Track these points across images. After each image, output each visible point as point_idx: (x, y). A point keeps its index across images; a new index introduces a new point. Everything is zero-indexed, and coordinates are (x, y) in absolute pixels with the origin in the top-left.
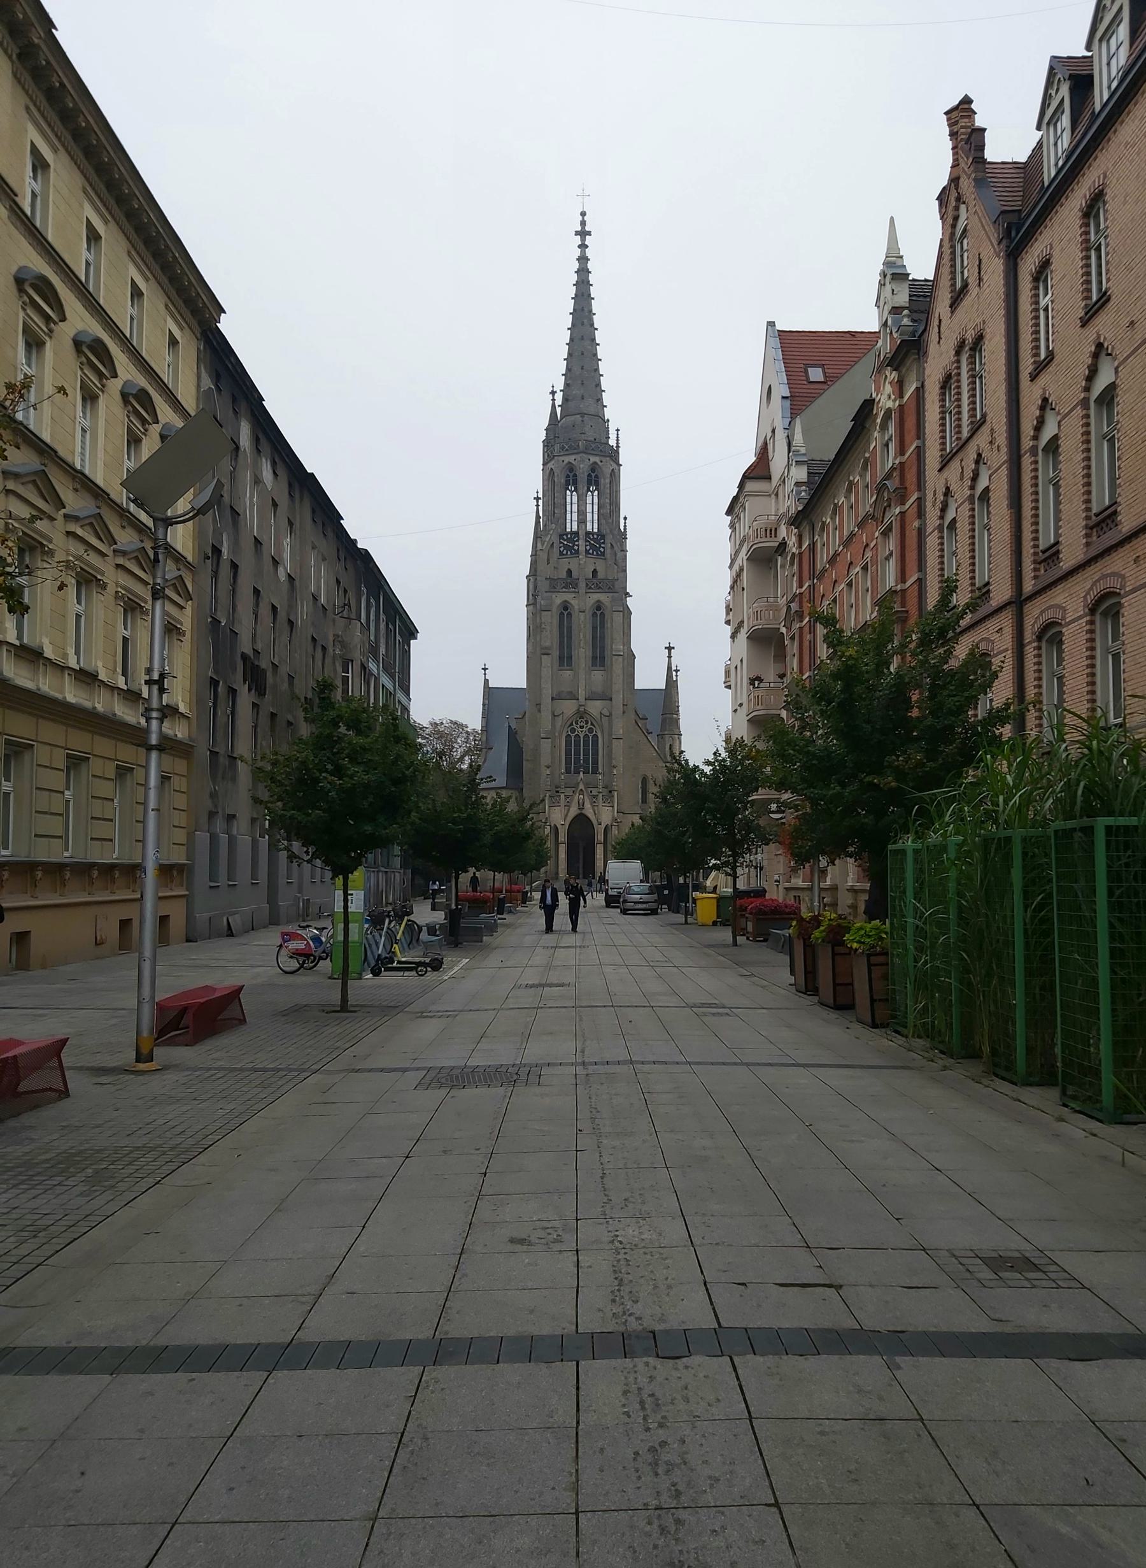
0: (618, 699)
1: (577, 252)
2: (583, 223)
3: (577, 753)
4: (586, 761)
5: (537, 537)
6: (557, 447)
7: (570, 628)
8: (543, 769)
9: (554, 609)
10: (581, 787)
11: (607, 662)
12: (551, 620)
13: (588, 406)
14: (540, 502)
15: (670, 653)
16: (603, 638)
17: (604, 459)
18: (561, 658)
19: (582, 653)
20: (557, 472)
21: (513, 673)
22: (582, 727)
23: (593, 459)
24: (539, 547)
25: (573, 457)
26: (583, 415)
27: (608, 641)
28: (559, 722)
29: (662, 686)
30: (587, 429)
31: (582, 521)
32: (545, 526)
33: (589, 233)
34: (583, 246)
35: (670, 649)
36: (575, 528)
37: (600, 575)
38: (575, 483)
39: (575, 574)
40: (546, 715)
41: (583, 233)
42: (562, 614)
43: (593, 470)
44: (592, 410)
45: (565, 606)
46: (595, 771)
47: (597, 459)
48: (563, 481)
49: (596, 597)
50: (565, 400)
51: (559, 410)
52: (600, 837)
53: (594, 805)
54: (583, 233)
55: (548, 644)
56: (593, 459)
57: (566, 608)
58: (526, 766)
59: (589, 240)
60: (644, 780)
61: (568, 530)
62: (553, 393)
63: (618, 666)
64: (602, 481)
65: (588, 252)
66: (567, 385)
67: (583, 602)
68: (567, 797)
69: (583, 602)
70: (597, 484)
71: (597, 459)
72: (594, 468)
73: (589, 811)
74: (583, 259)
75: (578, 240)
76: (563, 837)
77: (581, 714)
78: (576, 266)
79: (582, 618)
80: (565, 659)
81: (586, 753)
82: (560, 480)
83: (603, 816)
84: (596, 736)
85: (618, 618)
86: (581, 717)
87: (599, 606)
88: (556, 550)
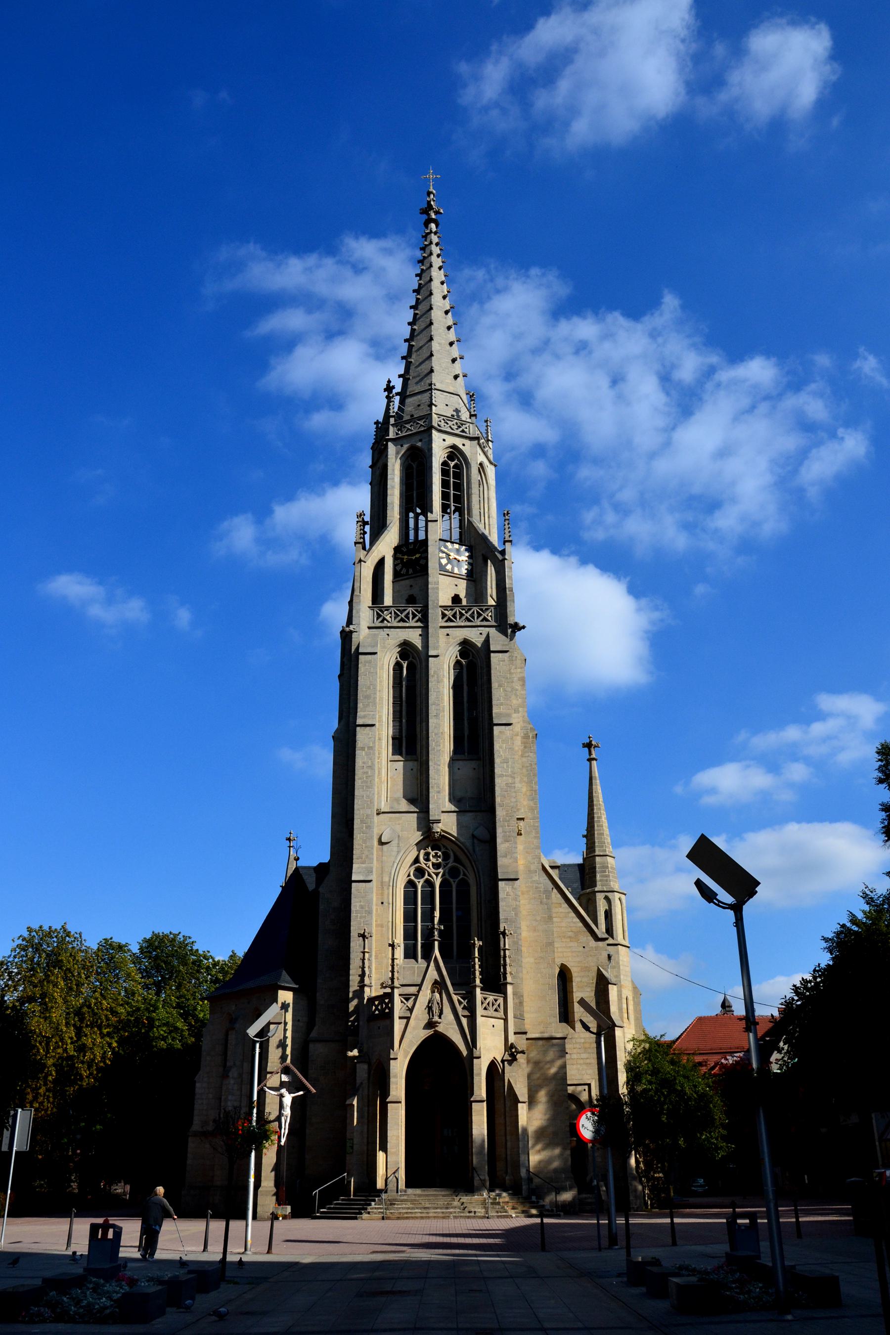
3: (428, 916)
14: (367, 528)
23: (451, 440)
43: (451, 457)
47: (458, 442)
49: (460, 634)
56: (451, 440)
60: (564, 976)
70: (458, 476)
71: (458, 442)
75: (425, 217)
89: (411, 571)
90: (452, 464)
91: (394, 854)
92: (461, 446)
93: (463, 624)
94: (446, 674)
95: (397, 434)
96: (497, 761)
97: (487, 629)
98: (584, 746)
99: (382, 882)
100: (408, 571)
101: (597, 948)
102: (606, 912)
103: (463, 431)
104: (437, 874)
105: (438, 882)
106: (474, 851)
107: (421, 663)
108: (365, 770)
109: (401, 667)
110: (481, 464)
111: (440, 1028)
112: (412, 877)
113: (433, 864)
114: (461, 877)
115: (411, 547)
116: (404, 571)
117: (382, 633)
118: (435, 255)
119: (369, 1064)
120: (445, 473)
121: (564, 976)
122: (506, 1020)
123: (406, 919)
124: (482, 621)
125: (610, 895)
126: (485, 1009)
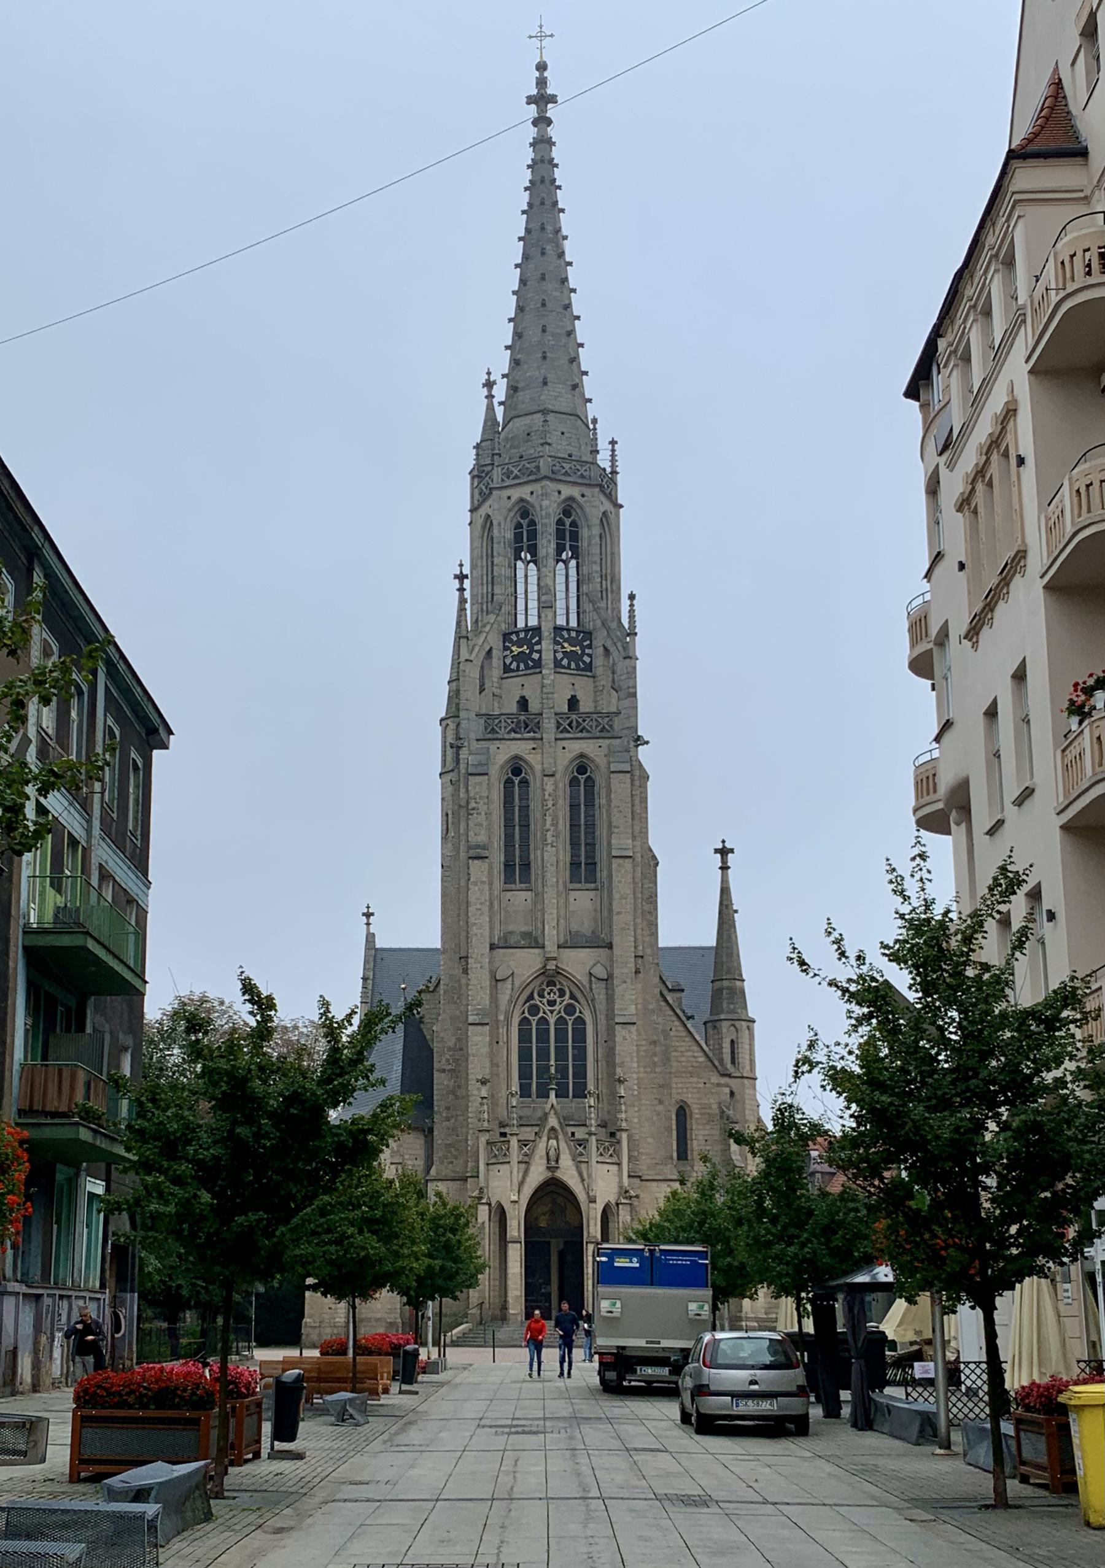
0: (624, 945)
1: (532, 132)
2: (542, 83)
3: (544, 1054)
4: (562, 1070)
5: (460, 637)
6: (497, 473)
7: (525, 810)
8: (473, 1086)
9: (494, 771)
10: (553, 1122)
11: (602, 875)
12: (489, 793)
13: (556, 397)
15: (724, 861)
16: (591, 827)
17: (588, 491)
18: (509, 866)
19: (552, 855)
20: (496, 518)
21: (416, 923)
22: (552, 1003)
23: (567, 491)
24: (464, 654)
25: (528, 489)
26: (545, 412)
27: (602, 831)
28: (505, 993)
29: (710, 940)
30: (553, 438)
31: (546, 606)
32: (476, 622)
33: (553, 99)
34: (541, 121)
35: (724, 852)
36: (533, 622)
37: (585, 706)
38: (533, 535)
39: (534, 707)
40: (479, 976)
41: (542, 99)
42: (509, 782)
43: (567, 512)
44: (563, 404)
45: (516, 767)
46: (581, 1092)
47: (575, 492)
48: (510, 535)
49: (576, 747)
50: (513, 389)
51: (499, 412)
52: (594, 1229)
53: (579, 1161)
54: (542, 99)
55: (482, 838)
56: (567, 491)
57: (517, 771)
58: (441, 1082)
59: (552, 111)
60: (682, 1113)
61: (521, 624)
62: (489, 385)
63: (622, 878)
64: (584, 533)
65: (552, 132)
66: (515, 363)
67: (551, 758)
68: (523, 1143)
69: (551, 758)
70: (575, 536)
71: (575, 492)
72: (568, 508)
73: (568, 1174)
74: (542, 143)
75: (532, 111)
76: (516, 1228)
77: (551, 977)
78: (529, 155)
79: (549, 788)
80: (518, 869)
81: (561, 1054)
82: (504, 533)
83: (600, 1185)
84: (580, 1021)
85: (620, 786)
86: (551, 983)
87: (582, 766)
88: (496, 662)
89: (522, 666)
90: (568, 521)
91: (509, 992)
92: (579, 498)
93: (579, 735)
94: (561, 793)
95: (503, 480)
96: (616, 896)
97: (607, 741)
98: (716, 851)
99: (497, 1021)
100: (518, 666)
101: (719, 1085)
102: (732, 1041)
103: (582, 476)
104: (552, 1012)
105: (552, 1021)
106: (591, 989)
107: (535, 779)
108: (479, 906)
109: (513, 782)
110: (604, 513)
111: (558, 1174)
112: (526, 1015)
113: (548, 1001)
114: (577, 1014)
115: (522, 635)
116: (514, 666)
117: (493, 746)
118: (547, 182)
119: (489, 1205)
120: (560, 534)
121: (682, 1113)
122: (619, 1164)
123: (521, 1058)
124: (601, 731)
125: (736, 1023)
126: (601, 1155)
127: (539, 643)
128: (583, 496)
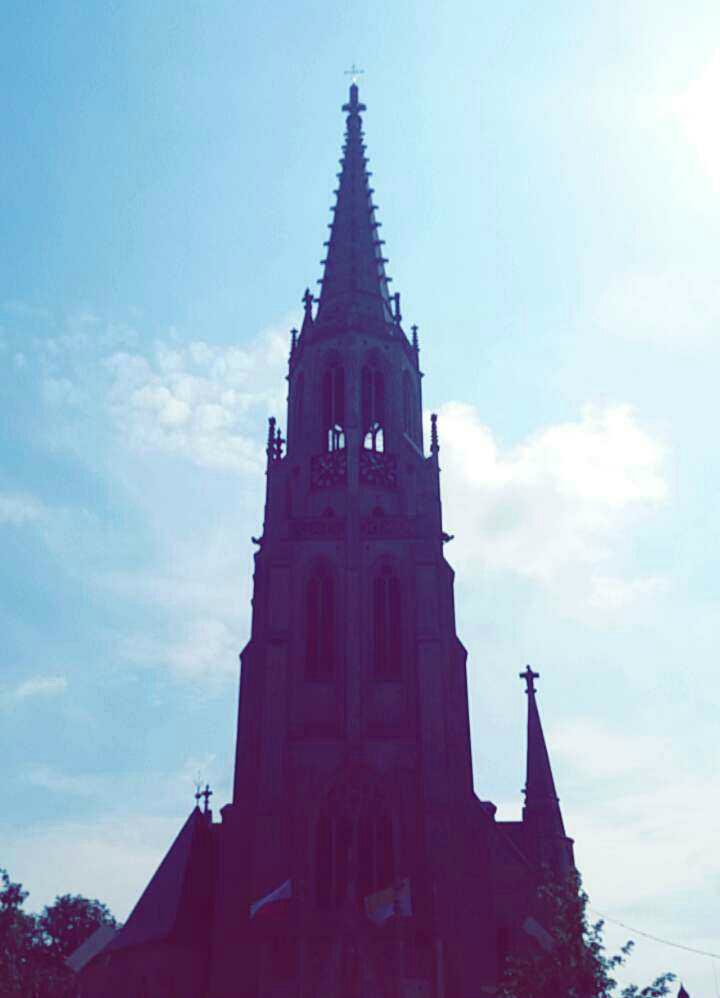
35: (530, 676)
61: (330, 449)
72: (373, 357)
78: (344, 128)
98: (522, 675)
127: (346, 459)
128: (387, 348)
